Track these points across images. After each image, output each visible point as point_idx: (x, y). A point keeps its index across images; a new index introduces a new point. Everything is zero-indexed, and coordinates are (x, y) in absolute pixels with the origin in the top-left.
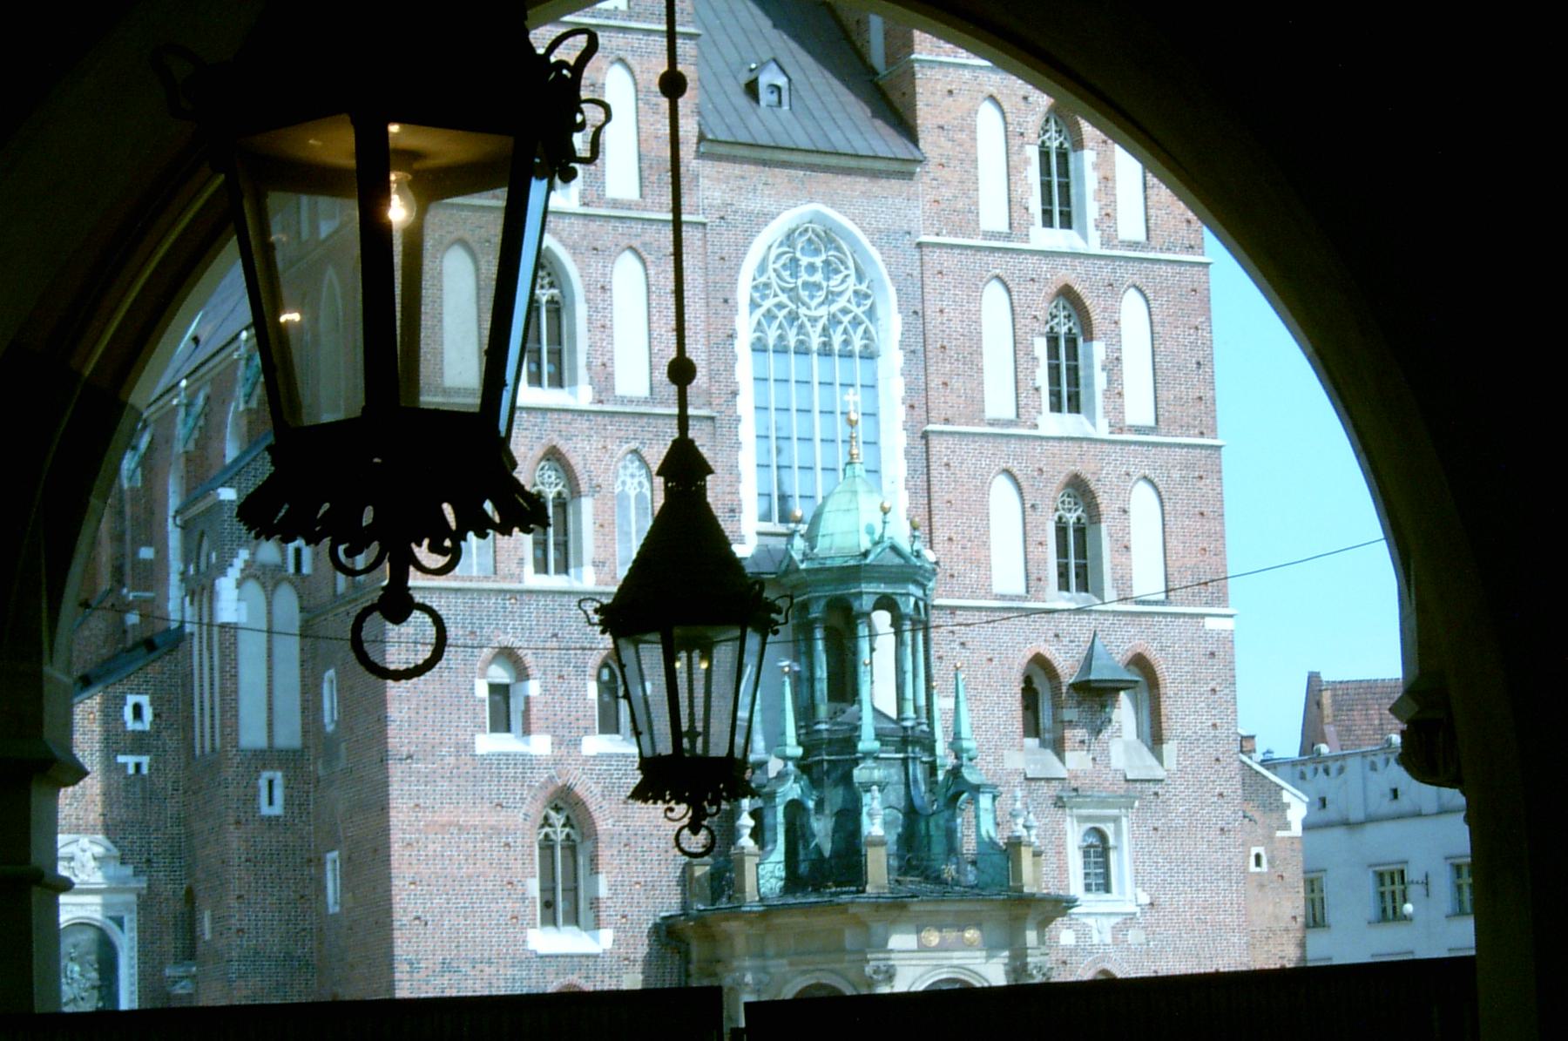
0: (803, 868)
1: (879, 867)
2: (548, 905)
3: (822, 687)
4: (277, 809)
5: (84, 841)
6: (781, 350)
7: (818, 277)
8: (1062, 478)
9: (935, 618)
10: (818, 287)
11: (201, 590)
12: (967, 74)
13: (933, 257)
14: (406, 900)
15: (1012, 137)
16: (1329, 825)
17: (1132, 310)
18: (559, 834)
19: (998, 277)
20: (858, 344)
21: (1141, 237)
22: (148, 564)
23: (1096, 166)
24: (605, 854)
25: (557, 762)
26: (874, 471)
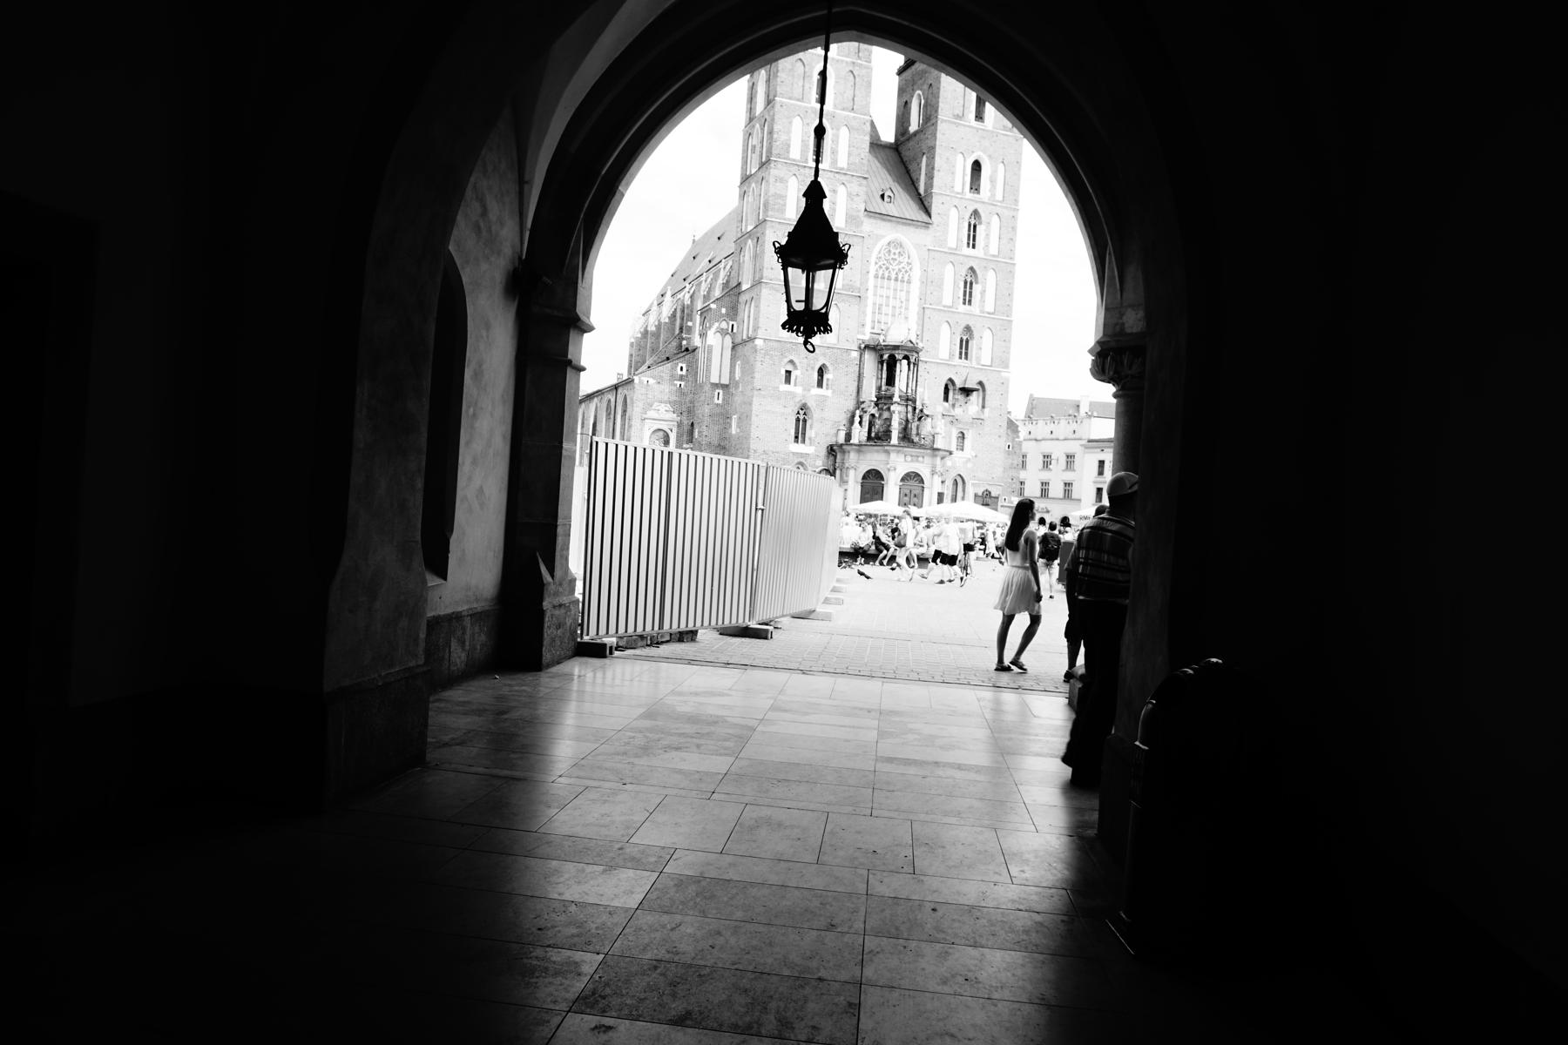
0: (873, 435)
1: (895, 439)
2: (797, 437)
3: (884, 381)
4: (720, 401)
5: (663, 405)
8: (964, 325)
9: (920, 364)
10: (896, 260)
11: (703, 335)
12: (948, 198)
13: (932, 253)
14: (754, 433)
15: (961, 218)
16: (1031, 440)
18: (801, 417)
19: (951, 262)
20: (906, 279)
21: (996, 253)
22: (690, 327)
24: (815, 424)
25: (804, 396)
26: (906, 318)
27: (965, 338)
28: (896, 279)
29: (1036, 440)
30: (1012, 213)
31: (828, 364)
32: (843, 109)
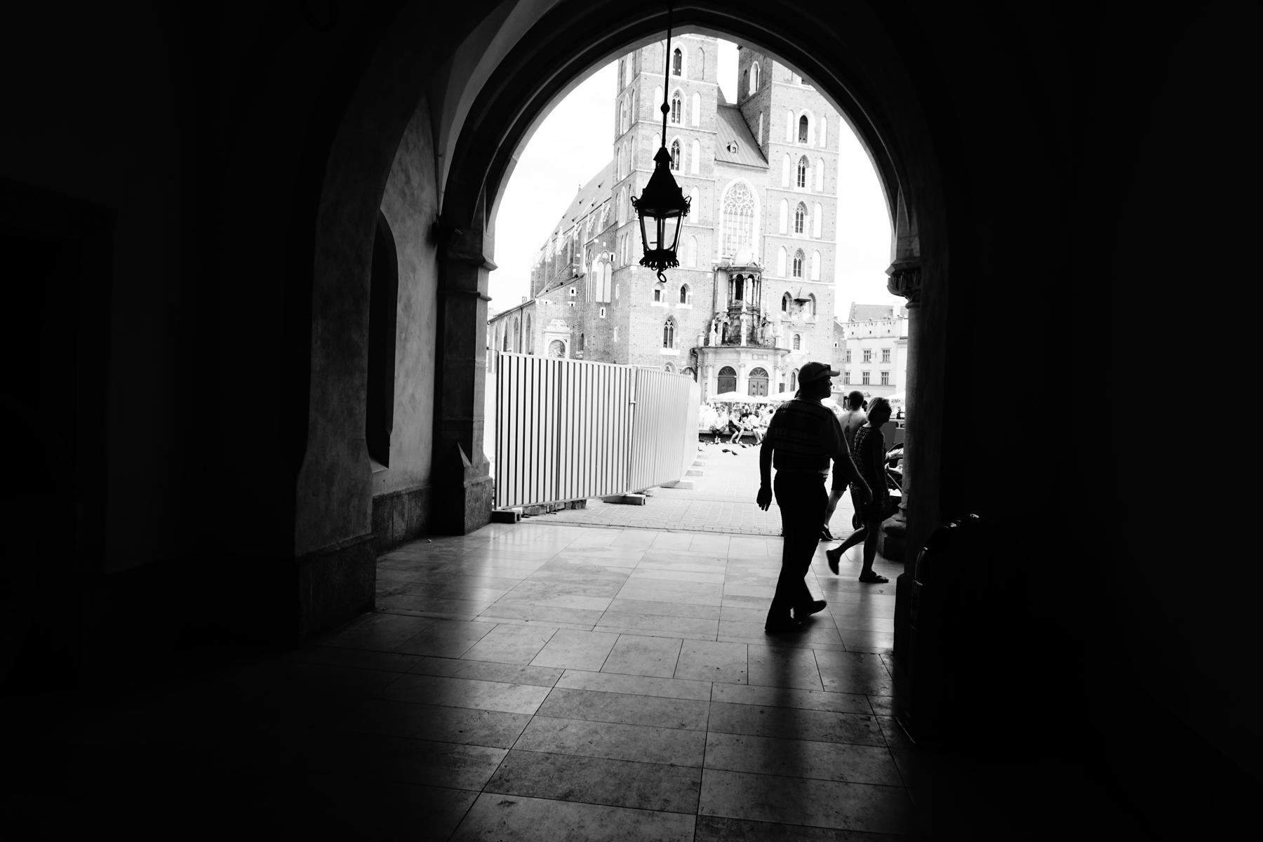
0: (726, 339)
1: (744, 342)
2: (665, 343)
3: (734, 296)
4: (604, 317)
5: (559, 321)
6: (731, 213)
7: (741, 196)
10: (741, 198)
11: (589, 264)
12: (782, 147)
13: (769, 192)
14: (632, 340)
16: (854, 339)
17: (818, 209)
18: (669, 327)
20: (749, 213)
21: (822, 190)
22: (579, 258)
23: (812, 172)
26: (750, 245)
27: (798, 259)
28: (742, 214)
29: (858, 339)
30: (833, 158)
31: (688, 284)
32: (696, 79)
